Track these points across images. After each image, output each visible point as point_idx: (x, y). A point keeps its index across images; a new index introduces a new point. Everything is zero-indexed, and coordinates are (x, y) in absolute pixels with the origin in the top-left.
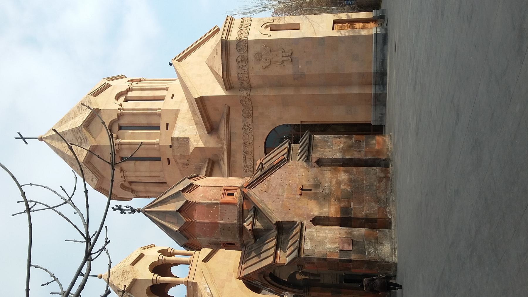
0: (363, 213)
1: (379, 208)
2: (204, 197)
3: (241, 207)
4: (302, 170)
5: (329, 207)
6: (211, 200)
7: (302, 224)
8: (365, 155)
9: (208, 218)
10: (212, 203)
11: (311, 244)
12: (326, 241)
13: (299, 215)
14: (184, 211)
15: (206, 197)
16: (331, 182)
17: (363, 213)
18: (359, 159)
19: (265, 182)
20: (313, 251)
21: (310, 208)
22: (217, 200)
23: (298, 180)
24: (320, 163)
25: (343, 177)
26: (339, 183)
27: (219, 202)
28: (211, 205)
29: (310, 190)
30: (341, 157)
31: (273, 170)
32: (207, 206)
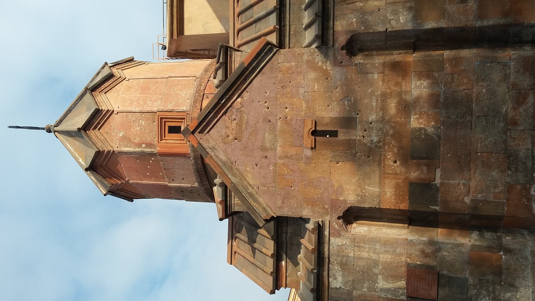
0: (467, 200)
1: (509, 188)
2: (126, 139)
3: (199, 161)
4: (312, 75)
5: (381, 184)
6: (140, 145)
7: (320, 228)
8: (481, 16)
9: (146, 177)
10: (143, 152)
11: (343, 276)
12: (376, 271)
13: (313, 203)
14: (101, 166)
15: (129, 140)
16: (384, 108)
17: (467, 200)
18: (462, 29)
19: (233, 114)
20: (350, 293)
21: (336, 185)
22: (149, 145)
23: (304, 105)
24: (355, 46)
25: (415, 93)
26: (407, 108)
27: (155, 151)
28: (142, 156)
29: (334, 134)
30: (409, 26)
31: (245, 80)
32: (137, 158)
